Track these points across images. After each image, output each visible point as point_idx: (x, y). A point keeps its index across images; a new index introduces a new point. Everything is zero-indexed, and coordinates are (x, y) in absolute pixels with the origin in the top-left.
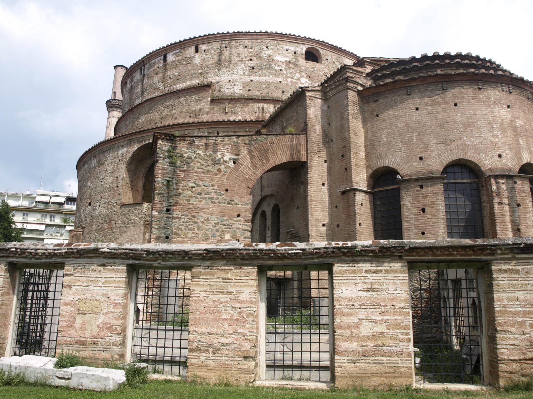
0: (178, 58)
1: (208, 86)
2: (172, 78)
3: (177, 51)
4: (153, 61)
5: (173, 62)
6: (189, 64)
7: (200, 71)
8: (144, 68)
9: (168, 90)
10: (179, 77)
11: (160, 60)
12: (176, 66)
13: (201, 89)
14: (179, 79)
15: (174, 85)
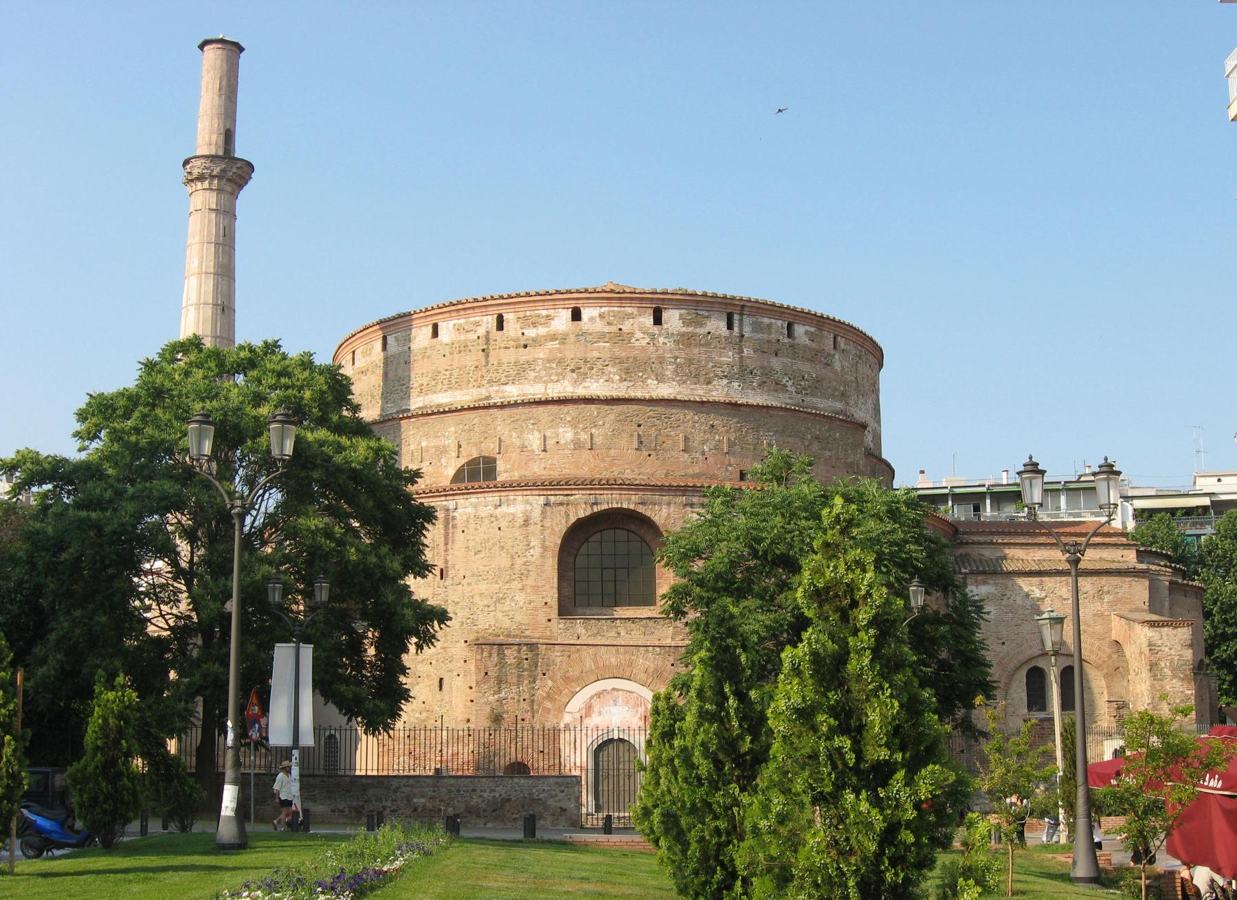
0: (814, 345)
1: (864, 426)
2: (807, 380)
3: (812, 329)
4: (766, 321)
5: (806, 346)
6: (827, 365)
7: (842, 389)
8: (741, 320)
9: (803, 400)
10: (817, 385)
11: (783, 328)
12: (811, 361)
13: (857, 429)
14: (816, 386)
15: (812, 395)
